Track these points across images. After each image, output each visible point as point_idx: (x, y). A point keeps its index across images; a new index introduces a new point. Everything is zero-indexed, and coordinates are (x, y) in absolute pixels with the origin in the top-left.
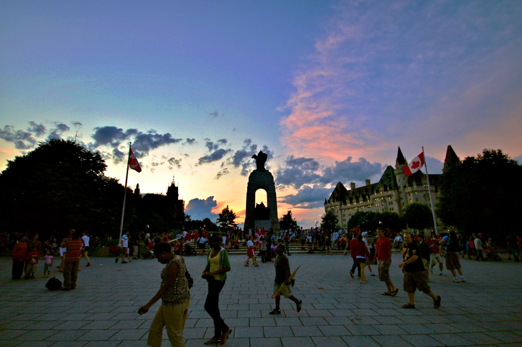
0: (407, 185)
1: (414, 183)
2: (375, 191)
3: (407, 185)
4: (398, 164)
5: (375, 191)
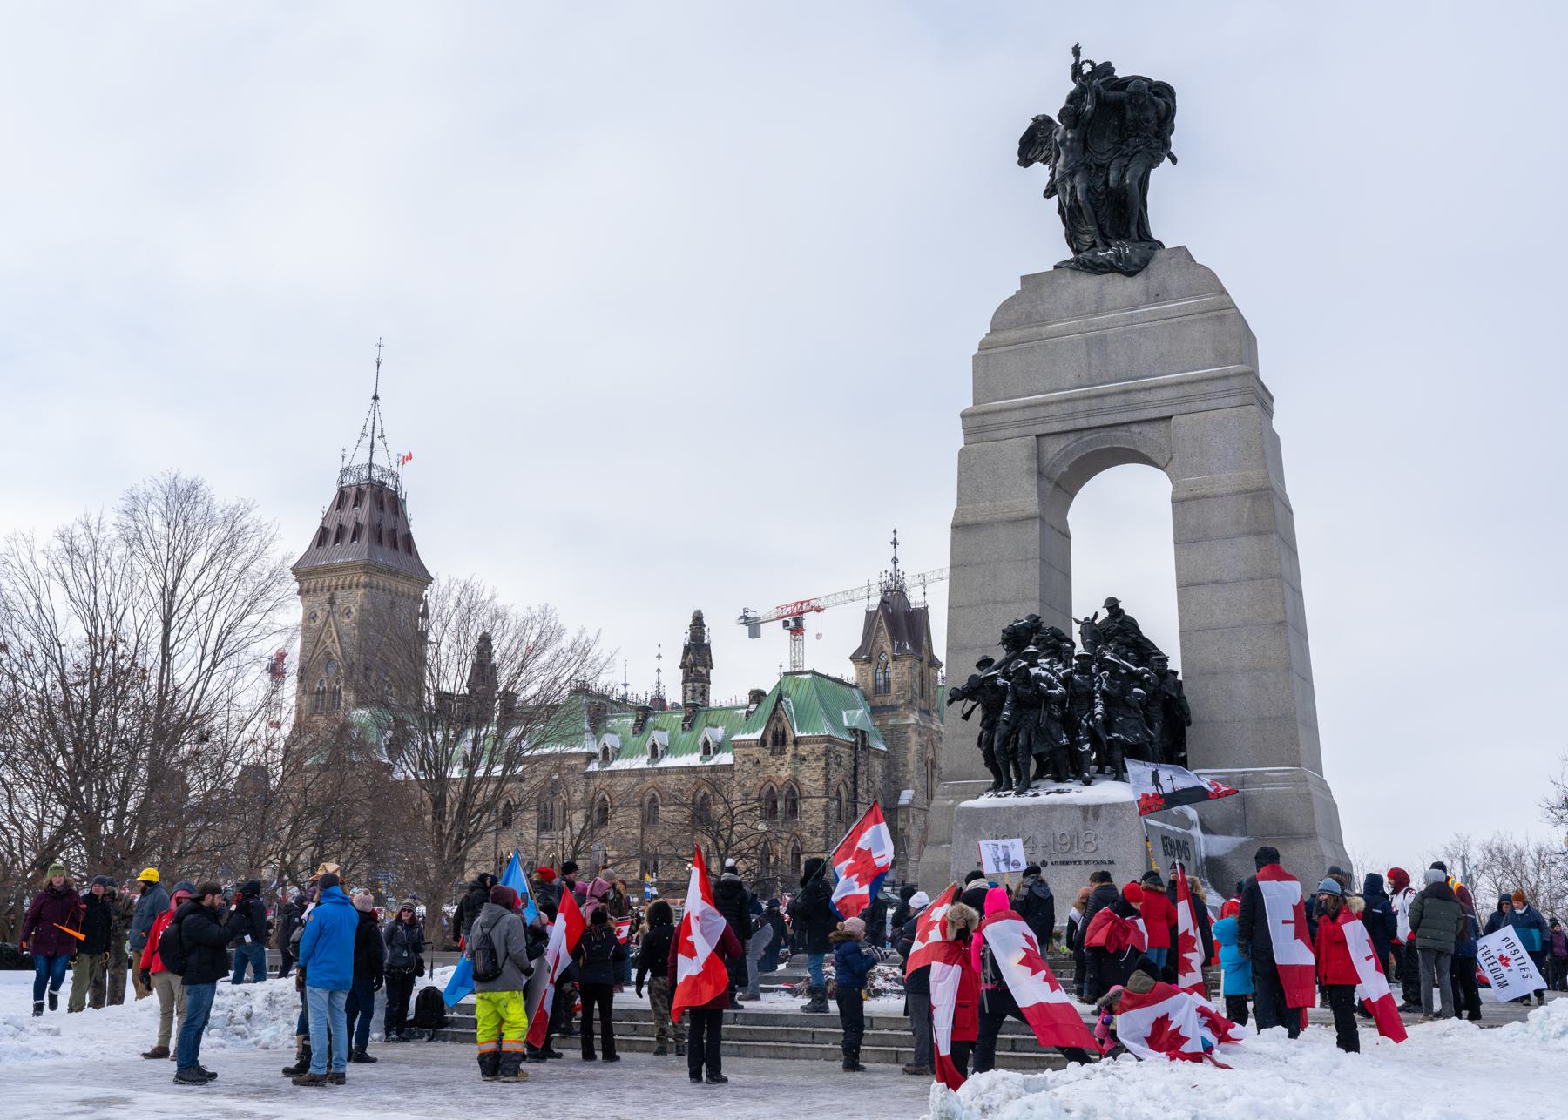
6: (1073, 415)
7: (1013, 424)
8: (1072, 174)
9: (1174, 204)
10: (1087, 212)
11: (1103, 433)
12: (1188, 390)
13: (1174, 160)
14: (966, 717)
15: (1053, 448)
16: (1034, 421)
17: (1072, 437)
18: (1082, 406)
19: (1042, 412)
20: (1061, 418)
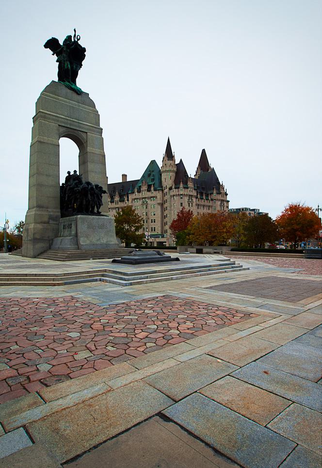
0: (173, 187)
1: (181, 185)
2: (136, 190)
3: (173, 187)
4: (166, 158)
5: (136, 190)
7: (53, 119)
8: (67, 61)
9: (82, 81)
11: (72, 130)
12: (91, 128)
15: (62, 130)
16: (58, 121)
17: (66, 128)
18: (69, 122)
19: (60, 119)
20: (64, 123)
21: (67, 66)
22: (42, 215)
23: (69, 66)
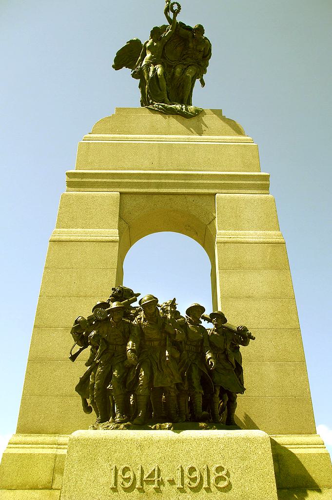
6: (149, 185)
10: (164, 84)
13: (203, 84)
14: (73, 358)
15: (130, 202)
16: (119, 185)
21: (155, 70)
22: (31, 456)
23: (159, 71)
